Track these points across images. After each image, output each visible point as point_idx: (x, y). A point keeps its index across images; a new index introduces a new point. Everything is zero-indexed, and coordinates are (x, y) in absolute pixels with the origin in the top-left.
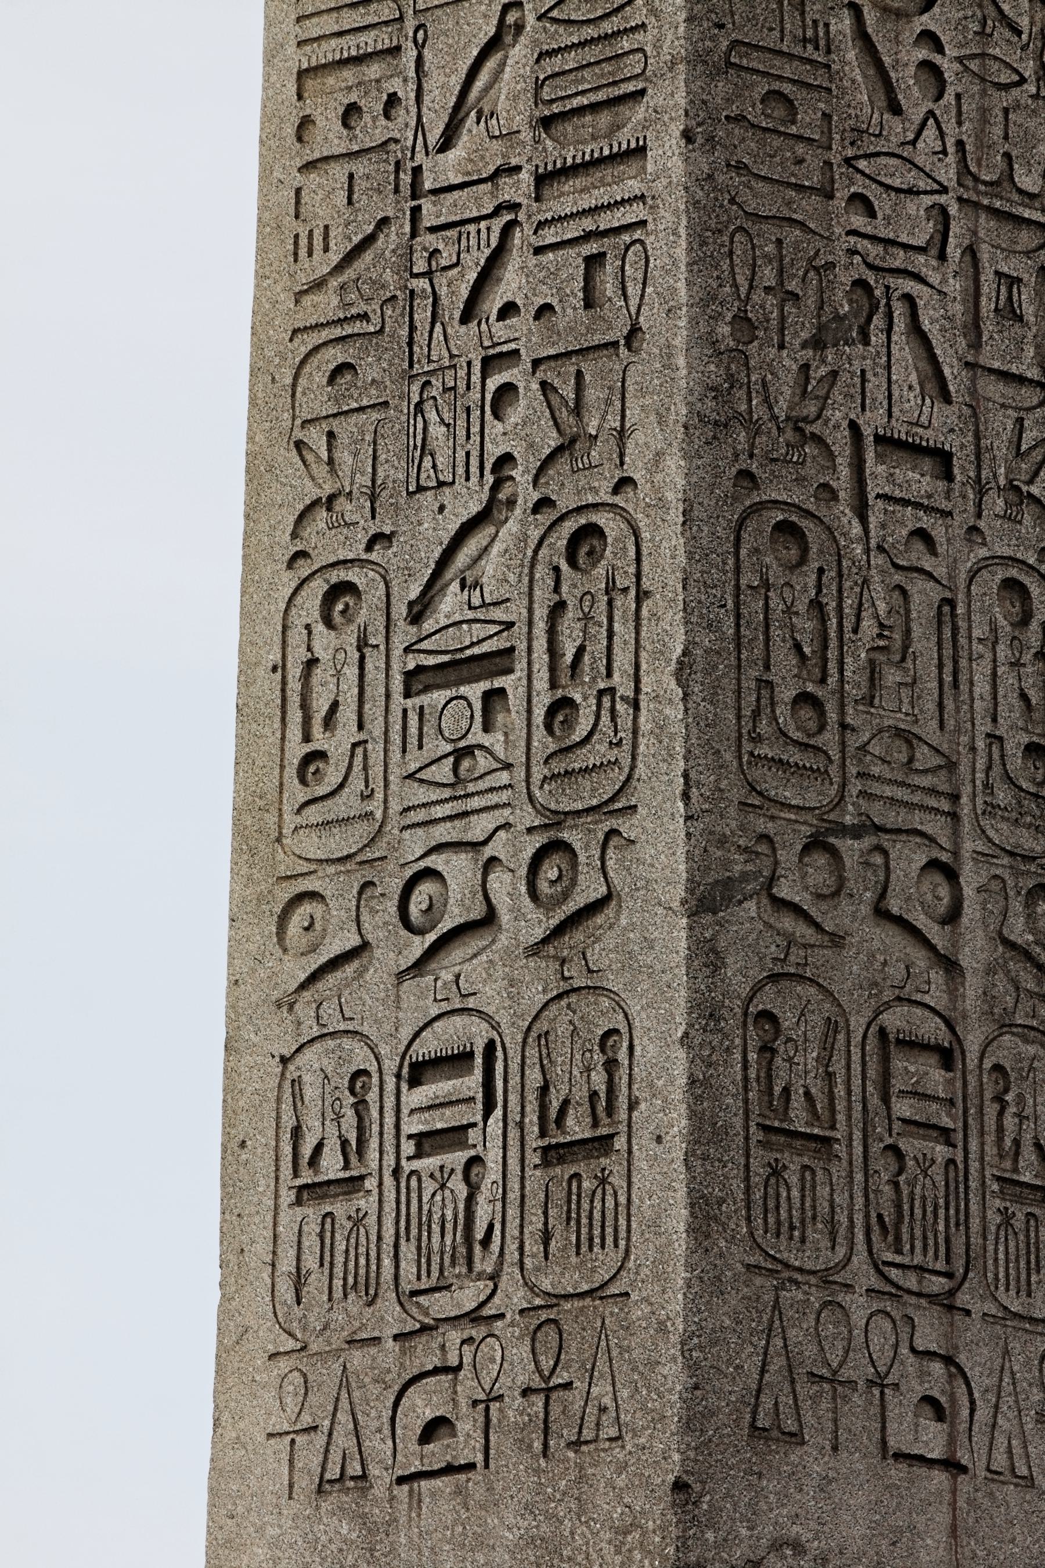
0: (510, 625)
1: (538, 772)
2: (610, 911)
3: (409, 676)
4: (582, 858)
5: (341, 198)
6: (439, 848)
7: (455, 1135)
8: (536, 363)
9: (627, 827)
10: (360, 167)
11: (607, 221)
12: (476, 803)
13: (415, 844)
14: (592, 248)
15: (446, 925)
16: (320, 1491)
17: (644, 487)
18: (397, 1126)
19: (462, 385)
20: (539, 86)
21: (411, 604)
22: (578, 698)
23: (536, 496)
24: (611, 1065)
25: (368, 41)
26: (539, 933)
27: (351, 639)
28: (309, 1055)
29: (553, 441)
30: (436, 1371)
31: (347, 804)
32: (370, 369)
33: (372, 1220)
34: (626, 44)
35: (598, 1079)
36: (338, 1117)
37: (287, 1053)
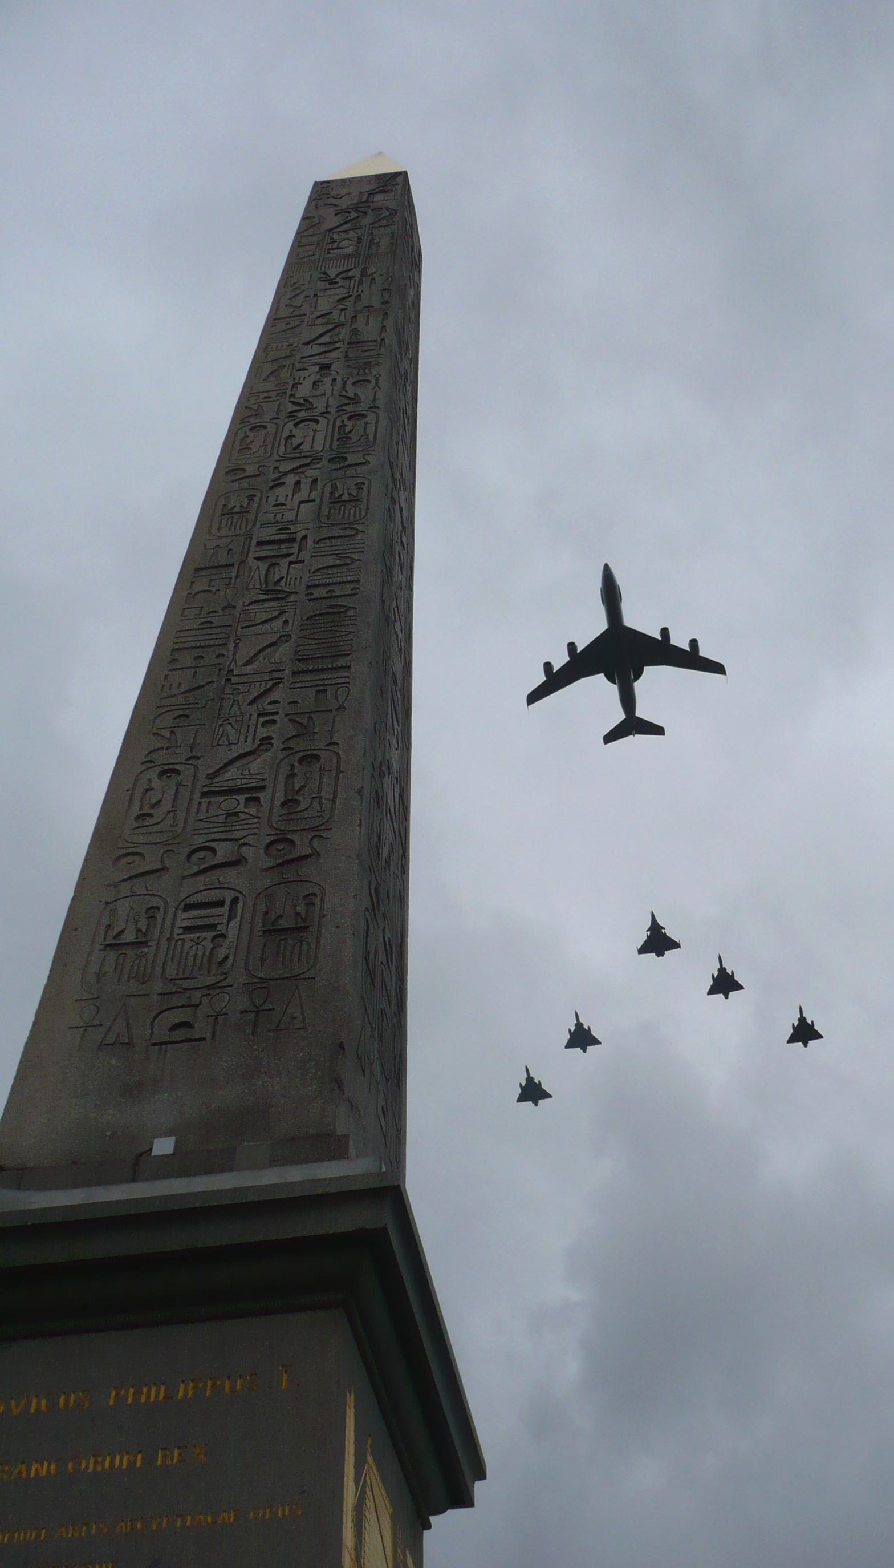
1: (274, 819)
6: (213, 841)
7: (212, 927)
16: (99, 1048)
20: (296, 652)
21: (208, 774)
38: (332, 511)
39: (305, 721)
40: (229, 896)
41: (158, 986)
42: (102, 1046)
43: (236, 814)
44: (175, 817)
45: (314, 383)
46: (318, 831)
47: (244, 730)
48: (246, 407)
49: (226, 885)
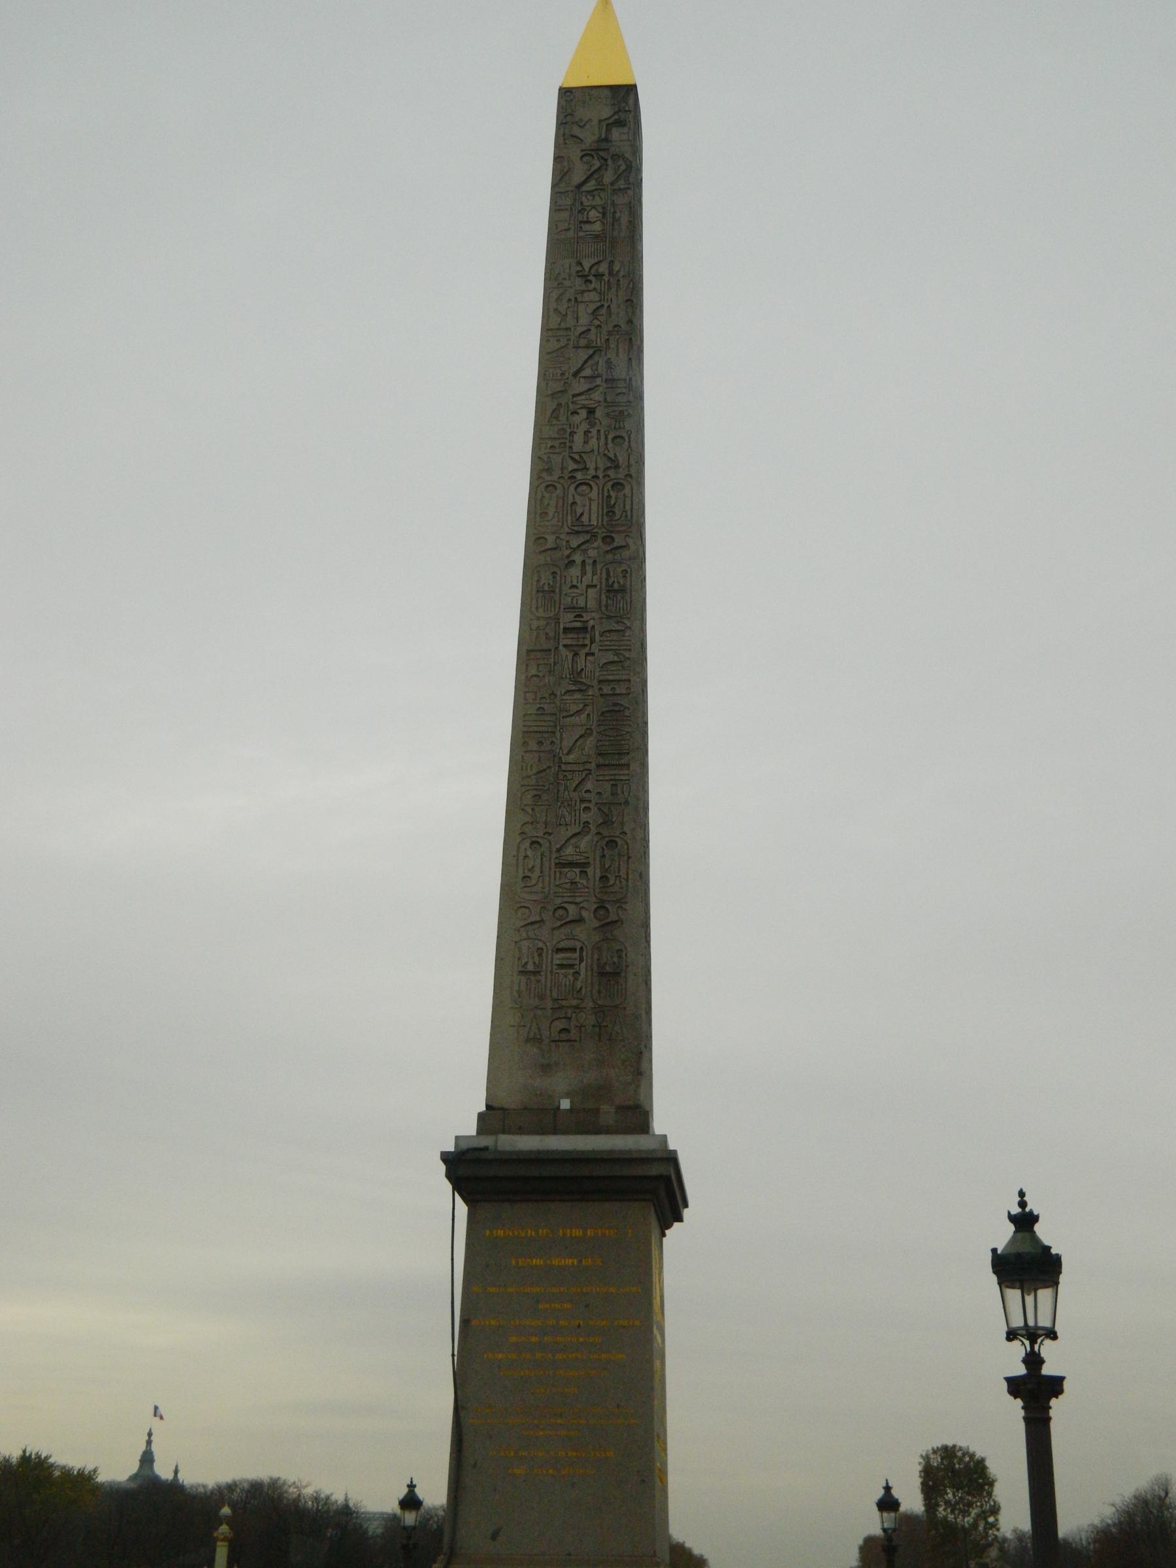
0: (588, 858)
1: (597, 890)
2: (619, 923)
3: (556, 864)
4: (611, 910)
5: (537, 760)
7: (571, 966)
8: (597, 803)
9: (624, 906)
10: (542, 755)
11: (617, 777)
12: (577, 894)
13: (558, 901)
14: (614, 782)
15: (568, 920)
17: (629, 835)
18: (552, 962)
19: (573, 805)
20: (597, 747)
21: (557, 849)
22: (609, 876)
23: (596, 831)
24: (620, 957)
25: (545, 729)
26: (597, 925)
27: (539, 854)
28: (525, 942)
29: (601, 821)
30: (563, 1018)
31: (534, 889)
32: (545, 797)
33: (543, 981)
34: (623, 742)
35: (615, 959)
36: (533, 958)
37: (517, 940)
38: (609, 601)
39: (606, 811)
40: (578, 945)
41: (549, 1004)
42: (528, 1040)
43: (575, 883)
44: (543, 882)
45: (585, 432)
46: (620, 902)
47: (573, 813)
48: (539, 458)
49: (576, 938)
